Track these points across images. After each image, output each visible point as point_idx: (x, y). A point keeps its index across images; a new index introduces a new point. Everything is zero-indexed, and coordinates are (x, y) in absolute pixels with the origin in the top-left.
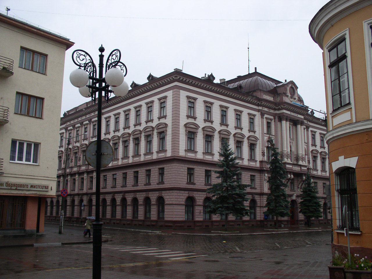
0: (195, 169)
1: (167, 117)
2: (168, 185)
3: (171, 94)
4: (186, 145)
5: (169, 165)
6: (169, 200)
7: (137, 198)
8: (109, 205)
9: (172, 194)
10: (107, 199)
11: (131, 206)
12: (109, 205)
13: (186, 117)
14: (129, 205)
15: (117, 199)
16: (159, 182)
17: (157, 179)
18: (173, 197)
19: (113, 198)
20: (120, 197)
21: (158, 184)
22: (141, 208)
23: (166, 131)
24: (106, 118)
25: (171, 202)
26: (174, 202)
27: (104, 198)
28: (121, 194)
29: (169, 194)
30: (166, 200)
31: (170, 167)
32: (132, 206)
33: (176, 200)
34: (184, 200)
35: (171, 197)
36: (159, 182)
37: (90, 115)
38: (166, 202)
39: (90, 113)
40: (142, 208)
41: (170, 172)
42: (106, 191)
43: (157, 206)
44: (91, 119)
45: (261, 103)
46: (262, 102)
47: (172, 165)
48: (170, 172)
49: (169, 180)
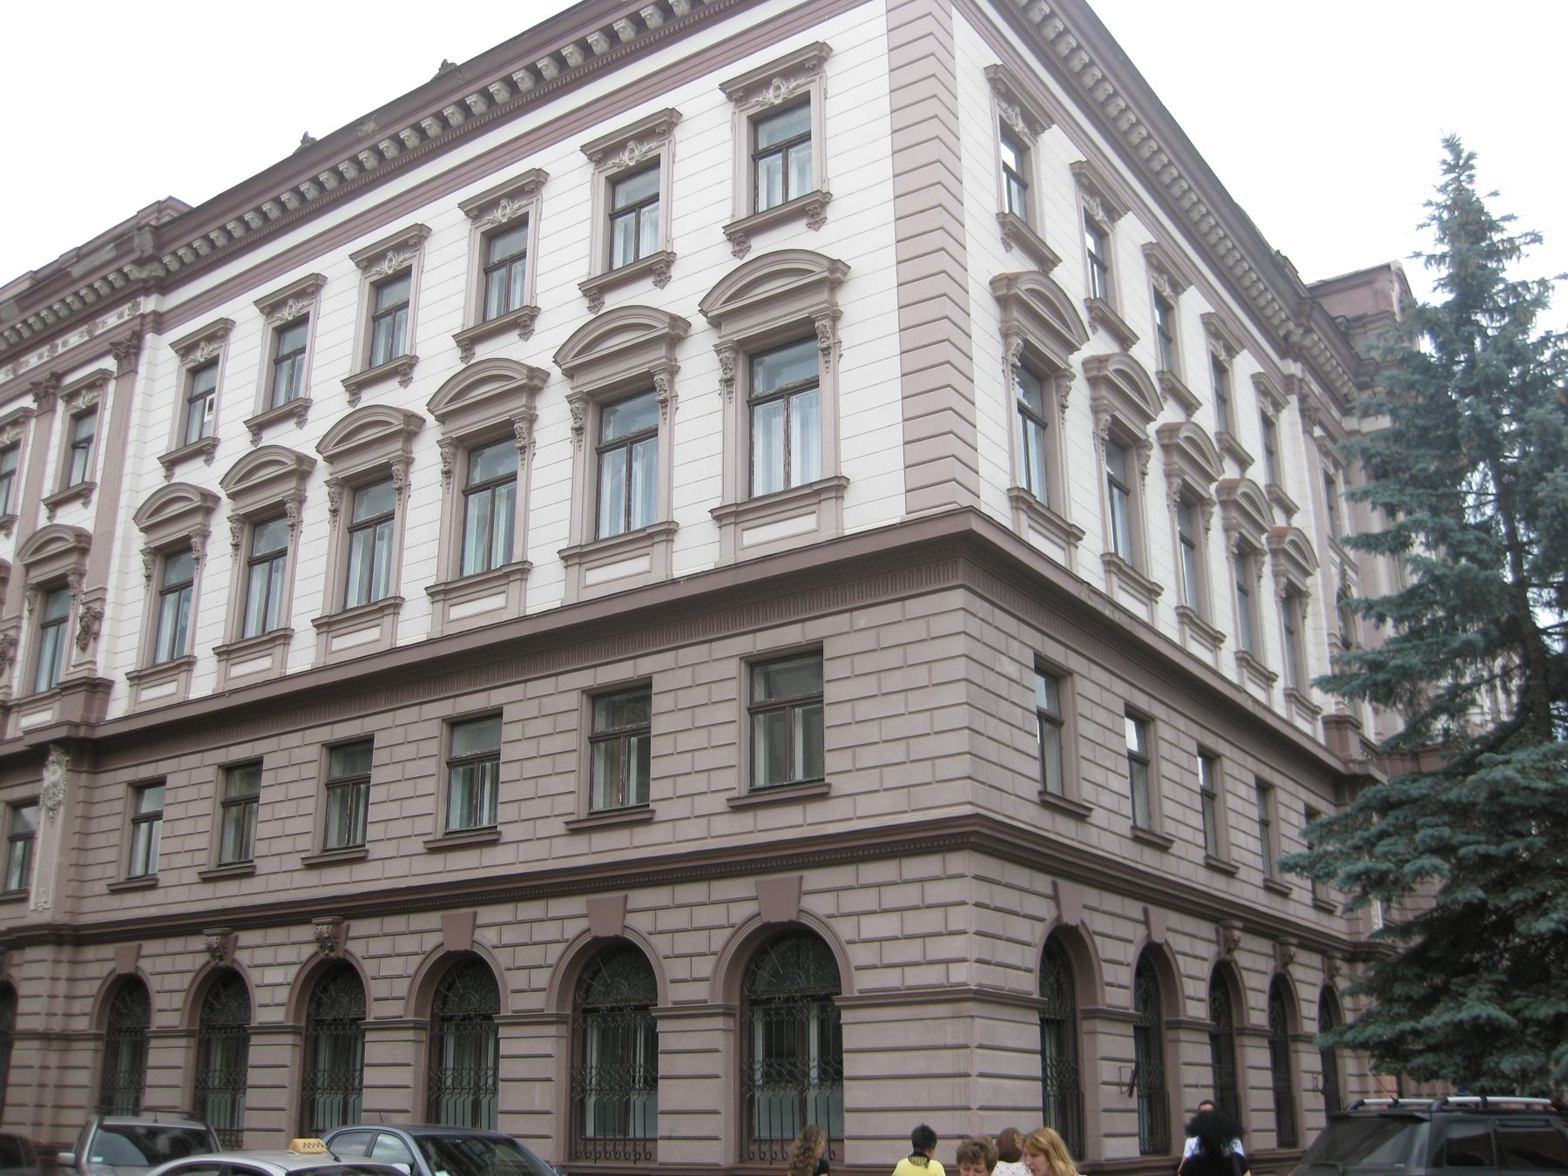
0: (1082, 686)
1: (832, 212)
2: (883, 803)
3: (881, 25)
4: (1012, 458)
5: (892, 612)
6: (894, 953)
7: (482, 962)
8: (168, 1033)
9: (937, 892)
10: (154, 984)
11: (410, 1035)
12: (168, 1033)
13: (997, 231)
14: (385, 1025)
15: (253, 977)
16: (754, 791)
17: (730, 756)
18: (958, 918)
19: (214, 971)
20: (287, 954)
21: (737, 807)
22: (547, 1046)
23: (836, 317)
24: (185, 348)
25: (890, 980)
26: (960, 975)
27: (125, 969)
28: (305, 932)
29: (893, 897)
30: (859, 955)
31: (890, 636)
32: (424, 1036)
33: (982, 948)
34: (1032, 958)
35: (931, 921)
36: (754, 791)
37: (54, 348)
38: (859, 982)
39: (48, 335)
40: (547, 1046)
41: (893, 682)
42: (153, 912)
43: (731, 1023)
44: (58, 377)
45: (1308, 331)
46: (1313, 325)
47: (915, 607)
48: (893, 682)
49: (896, 753)
